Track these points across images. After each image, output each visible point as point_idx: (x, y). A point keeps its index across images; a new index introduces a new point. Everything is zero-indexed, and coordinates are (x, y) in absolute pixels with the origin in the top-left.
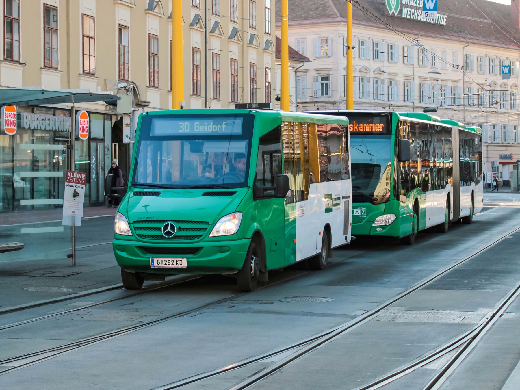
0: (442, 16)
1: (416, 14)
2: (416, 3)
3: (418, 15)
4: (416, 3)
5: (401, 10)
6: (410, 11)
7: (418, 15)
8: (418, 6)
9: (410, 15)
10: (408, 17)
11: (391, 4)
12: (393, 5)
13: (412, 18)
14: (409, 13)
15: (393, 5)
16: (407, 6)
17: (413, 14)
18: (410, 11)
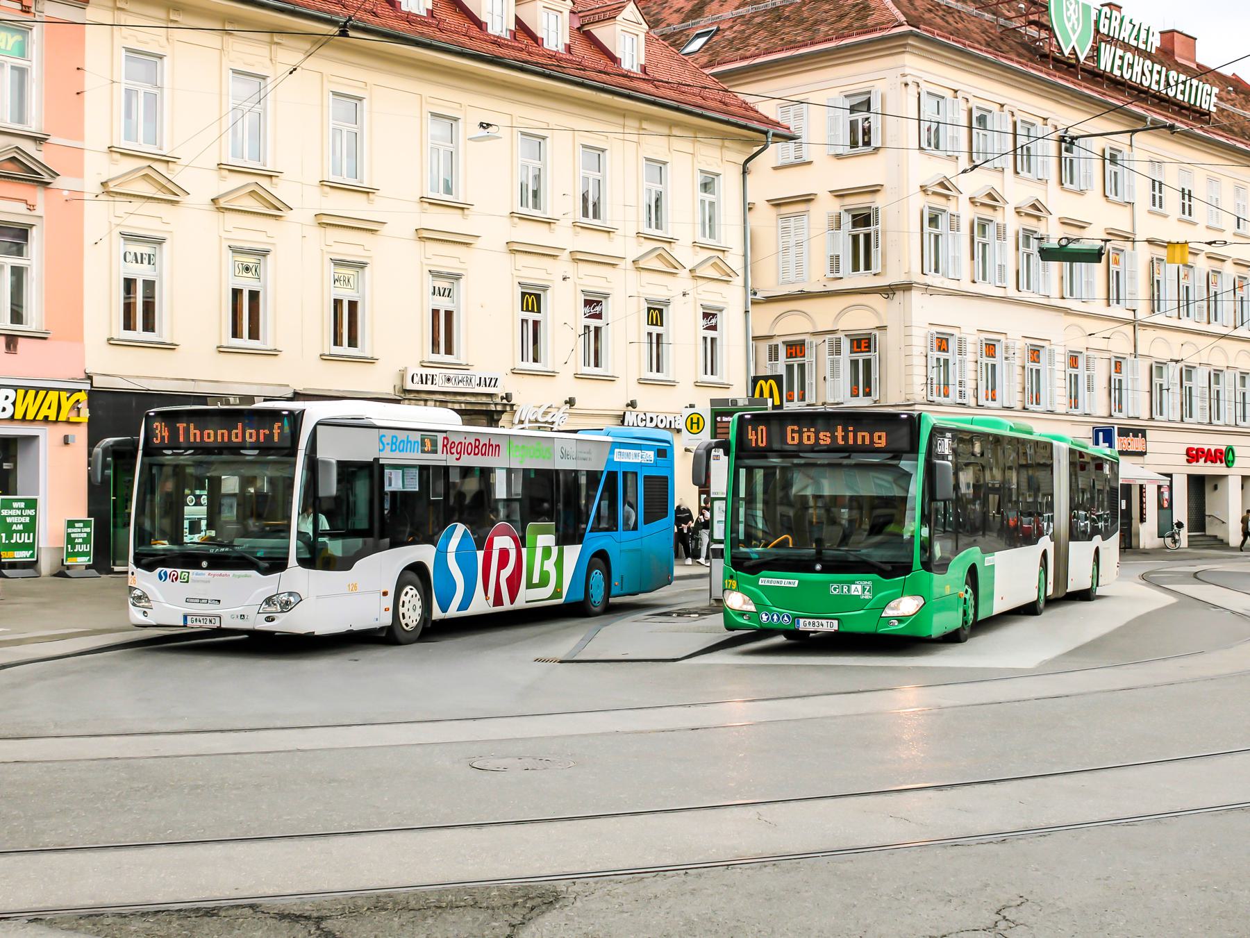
0: (1207, 87)
1: (1138, 69)
2: (1137, 38)
3: (1143, 74)
4: (1137, 38)
5: (1096, 49)
6: (1122, 58)
7: (1143, 74)
8: (1142, 46)
9: (1121, 68)
10: (1117, 72)
11: (1069, 26)
12: (1074, 32)
13: (1127, 76)
14: (1118, 62)
15: (1074, 32)
16: (1111, 40)
17: (1131, 66)
18: (1122, 58)
